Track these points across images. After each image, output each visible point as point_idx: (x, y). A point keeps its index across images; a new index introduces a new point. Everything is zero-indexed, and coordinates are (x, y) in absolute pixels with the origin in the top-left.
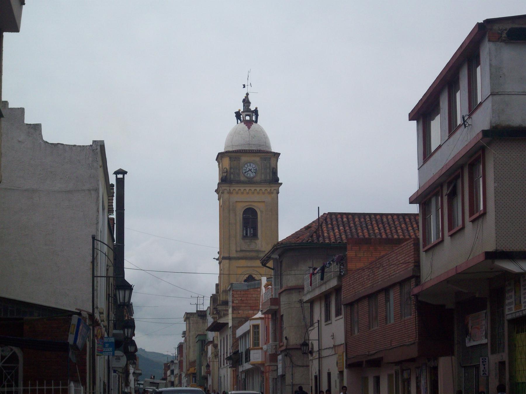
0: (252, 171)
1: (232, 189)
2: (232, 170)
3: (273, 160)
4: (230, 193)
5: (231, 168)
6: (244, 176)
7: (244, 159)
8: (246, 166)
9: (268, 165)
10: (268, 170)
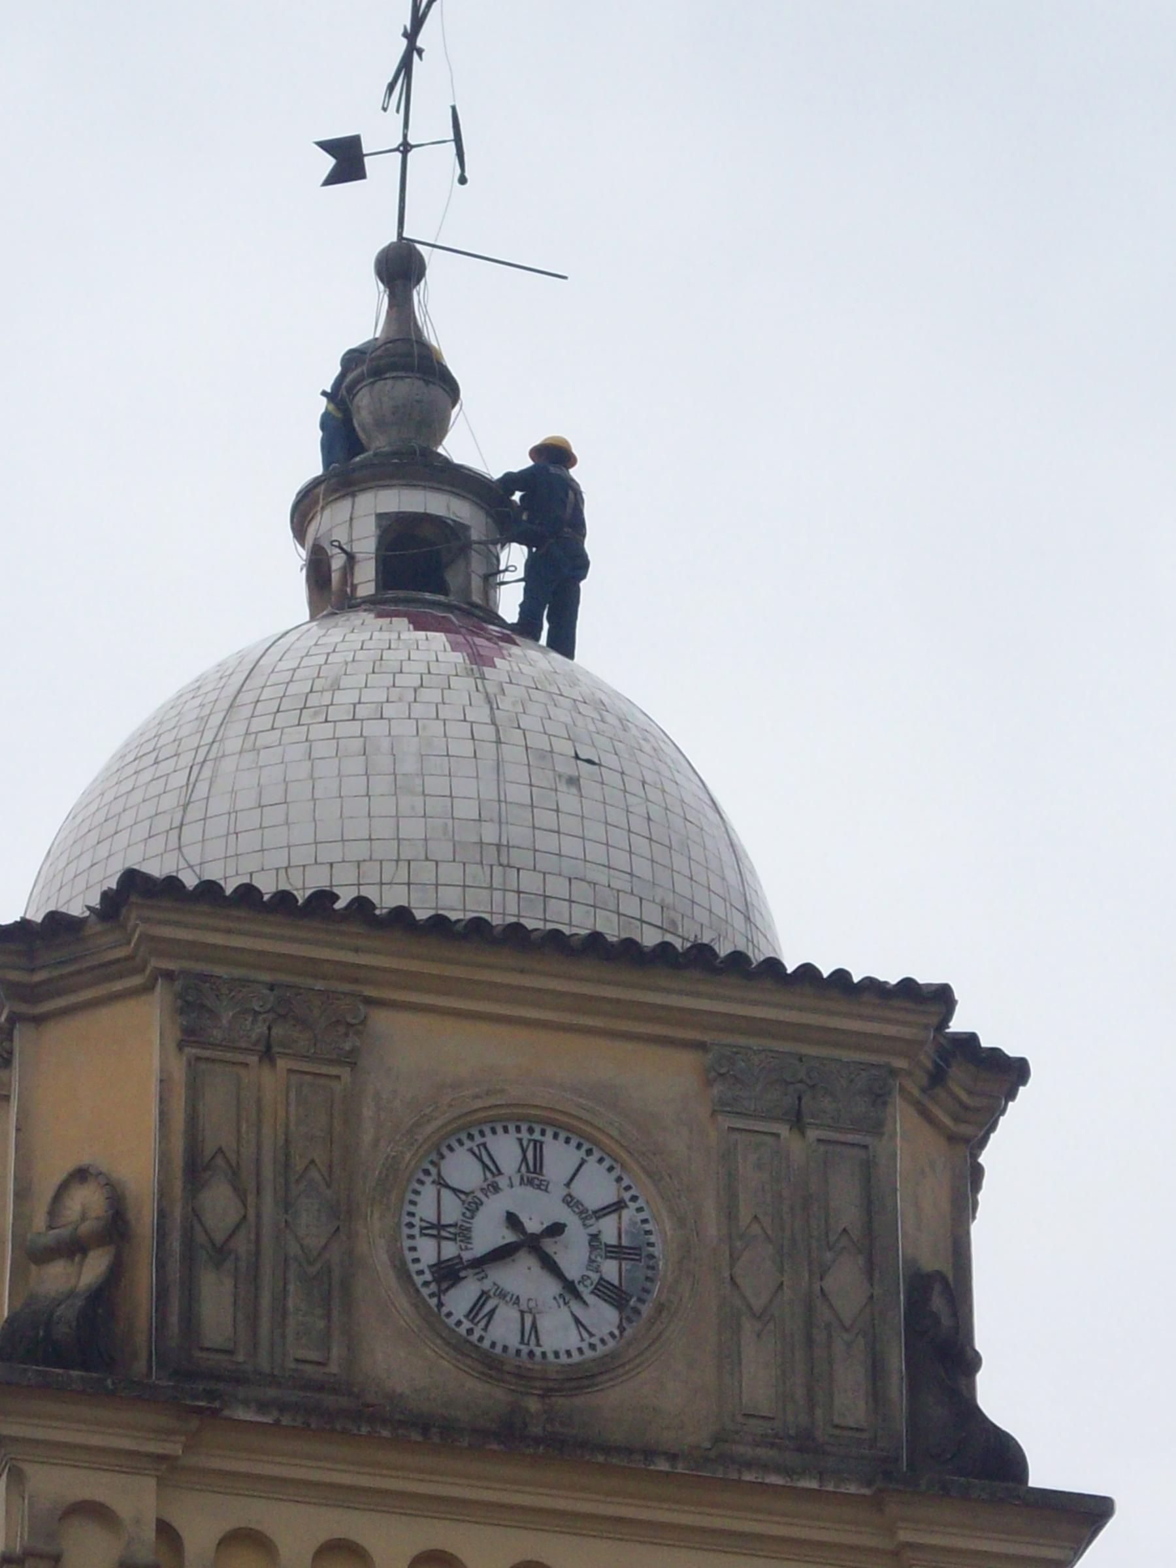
0: (573, 1256)
2: (220, 1205)
3: (907, 1141)
5: (196, 1167)
7: (422, 1051)
8: (462, 1169)
10: (846, 1283)
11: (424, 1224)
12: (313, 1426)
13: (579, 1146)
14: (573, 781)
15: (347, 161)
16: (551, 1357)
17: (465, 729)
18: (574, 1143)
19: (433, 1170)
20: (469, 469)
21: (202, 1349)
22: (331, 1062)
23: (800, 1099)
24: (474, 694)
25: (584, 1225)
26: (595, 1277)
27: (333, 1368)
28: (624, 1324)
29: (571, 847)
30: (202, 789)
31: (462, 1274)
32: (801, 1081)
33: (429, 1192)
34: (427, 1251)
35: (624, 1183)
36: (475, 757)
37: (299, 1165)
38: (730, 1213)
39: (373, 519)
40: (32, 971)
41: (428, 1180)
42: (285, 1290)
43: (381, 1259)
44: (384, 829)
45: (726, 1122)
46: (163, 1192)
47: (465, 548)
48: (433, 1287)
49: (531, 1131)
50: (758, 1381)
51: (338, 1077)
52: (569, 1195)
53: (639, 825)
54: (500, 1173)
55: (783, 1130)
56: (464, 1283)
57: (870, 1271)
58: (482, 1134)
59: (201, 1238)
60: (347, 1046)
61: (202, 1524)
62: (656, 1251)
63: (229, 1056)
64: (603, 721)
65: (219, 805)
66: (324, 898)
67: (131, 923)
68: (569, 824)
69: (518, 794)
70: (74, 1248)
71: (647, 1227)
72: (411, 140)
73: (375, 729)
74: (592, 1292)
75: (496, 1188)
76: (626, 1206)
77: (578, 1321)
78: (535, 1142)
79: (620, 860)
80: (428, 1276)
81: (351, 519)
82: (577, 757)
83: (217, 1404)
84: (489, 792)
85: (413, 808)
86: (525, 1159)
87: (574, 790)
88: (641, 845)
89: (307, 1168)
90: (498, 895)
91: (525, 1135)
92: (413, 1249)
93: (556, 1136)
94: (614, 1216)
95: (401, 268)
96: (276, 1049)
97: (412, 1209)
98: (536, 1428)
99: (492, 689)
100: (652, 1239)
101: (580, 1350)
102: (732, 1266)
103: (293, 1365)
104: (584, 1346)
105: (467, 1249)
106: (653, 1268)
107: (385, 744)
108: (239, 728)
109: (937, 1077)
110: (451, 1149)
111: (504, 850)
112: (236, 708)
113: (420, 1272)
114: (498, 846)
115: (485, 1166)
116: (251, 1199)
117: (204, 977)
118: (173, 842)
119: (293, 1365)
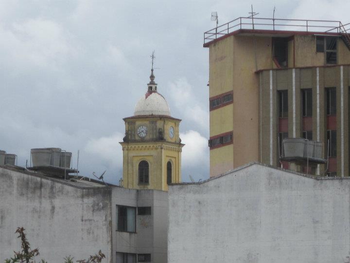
0: (144, 132)
1: (130, 147)
4: (127, 150)
6: (138, 136)
7: (138, 123)
9: (155, 127)
50: (151, 136)
98: (143, 140)
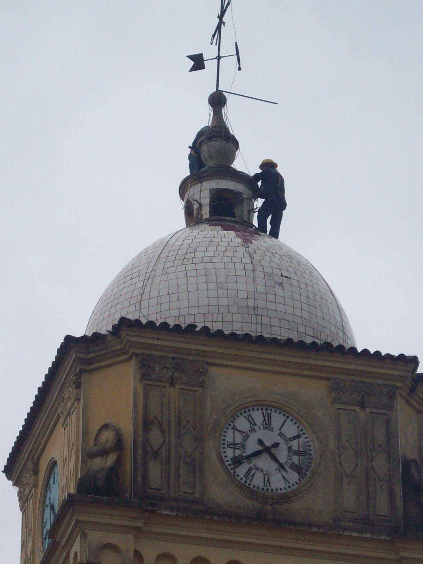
0: (282, 455)
2: (155, 437)
5: (147, 423)
7: (227, 381)
8: (242, 423)
10: (380, 463)
11: (229, 444)
12: (190, 516)
13: (284, 415)
14: (281, 284)
15: (198, 62)
16: (275, 491)
17: (242, 266)
18: (282, 414)
19: (232, 424)
20: (243, 173)
21: (150, 488)
22: (195, 386)
23: (363, 397)
24: (245, 253)
25: (286, 443)
26: (290, 462)
27: (196, 495)
28: (301, 479)
29: (280, 308)
30: (148, 289)
31: (242, 461)
32: (364, 391)
33: (230, 432)
34: (230, 453)
35: (301, 428)
36: (246, 276)
37: (184, 423)
38: (338, 438)
39: (208, 190)
40: (88, 354)
41: (230, 427)
42: (179, 468)
43: (214, 456)
44: (213, 302)
45: (336, 406)
46: (135, 432)
47: (241, 201)
48: (232, 466)
49: (267, 410)
50: (349, 498)
51: (198, 391)
52: (281, 432)
53: (304, 299)
54: (256, 425)
55: (357, 409)
56: (243, 465)
57: (389, 460)
58: (249, 411)
59: (149, 449)
60: (201, 380)
61: (150, 551)
62: (312, 452)
63: (158, 384)
64: (291, 263)
65: (154, 294)
66: (192, 327)
67: (123, 337)
68: (280, 300)
69: (261, 289)
70: (103, 453)
71: (309, 444)
72: (221, 55)
73: (210, 266)
74: (289, 467)
75: (254, 430)
76: (301, 437)
77: (284, 478)
78: (268, 413)
79: (298, 312)
80: (230, 462)
81: (201, 191)
82: (282, 275)
83: (155, 509)
84: (250, 288)
85: (224, 295)
86: (264, 420)
87: (281, 288)
88: (305, 307)
89: (186, 424)
90: (254, 326)
91: (264, 411)
92: (225, 452)
93: (276, 412)
94: (296, 441)
95: (217, 101)
96: (175, 381)
97: (224, 438)
98: (269, 516)
99: (251, 251)
100: (311, 448)
101: (285, 489)
102: (340, 457)
103: (182, 494)
104: (287, 487)
105: (244, 452)
106: (310, 459)
107: (213, 272)
108: (160, 266)
109: (413, 389)
110: (238, 416)
111: (256, 309)
112: (160, 259)
113: (227, 461)
114: (254, 308)
115: (250, 422)
116: (167, 435)
117: (148, 355)
118: (138, 308)
119: (182, 494)
